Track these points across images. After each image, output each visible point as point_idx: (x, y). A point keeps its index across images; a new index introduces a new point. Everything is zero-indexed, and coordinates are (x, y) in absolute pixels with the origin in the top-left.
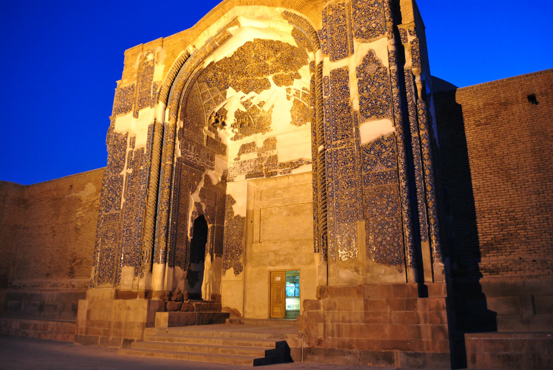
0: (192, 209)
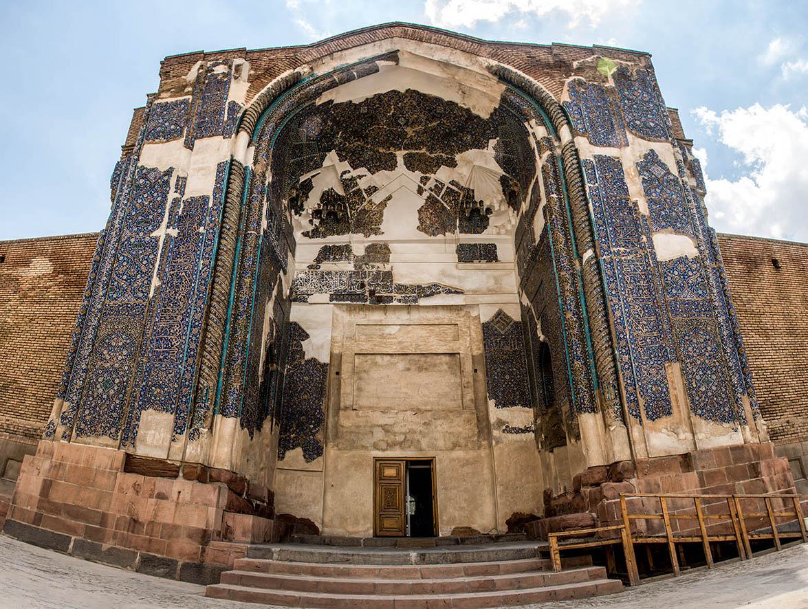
0: (266, 329)
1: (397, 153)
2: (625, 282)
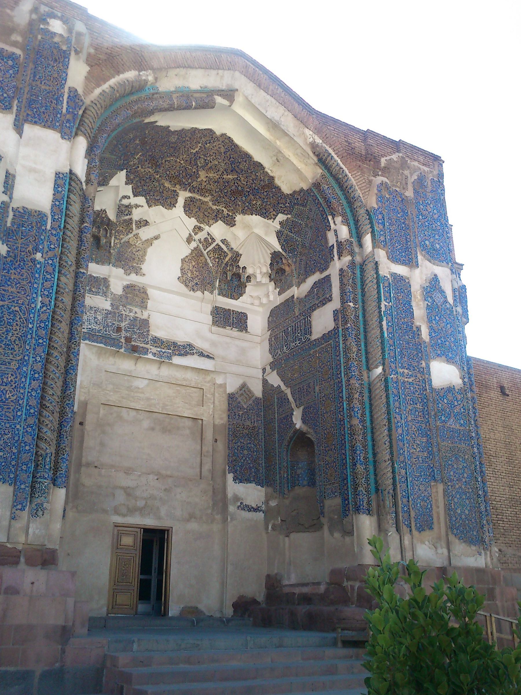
2: (406, 403)
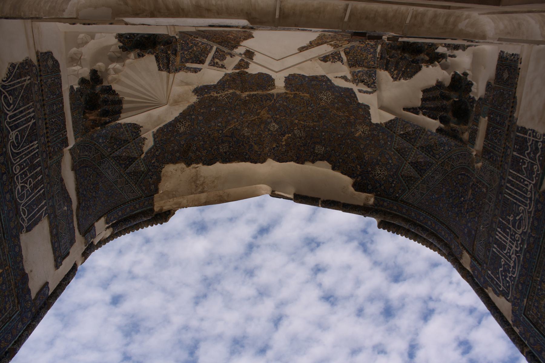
1: (283, 91)
